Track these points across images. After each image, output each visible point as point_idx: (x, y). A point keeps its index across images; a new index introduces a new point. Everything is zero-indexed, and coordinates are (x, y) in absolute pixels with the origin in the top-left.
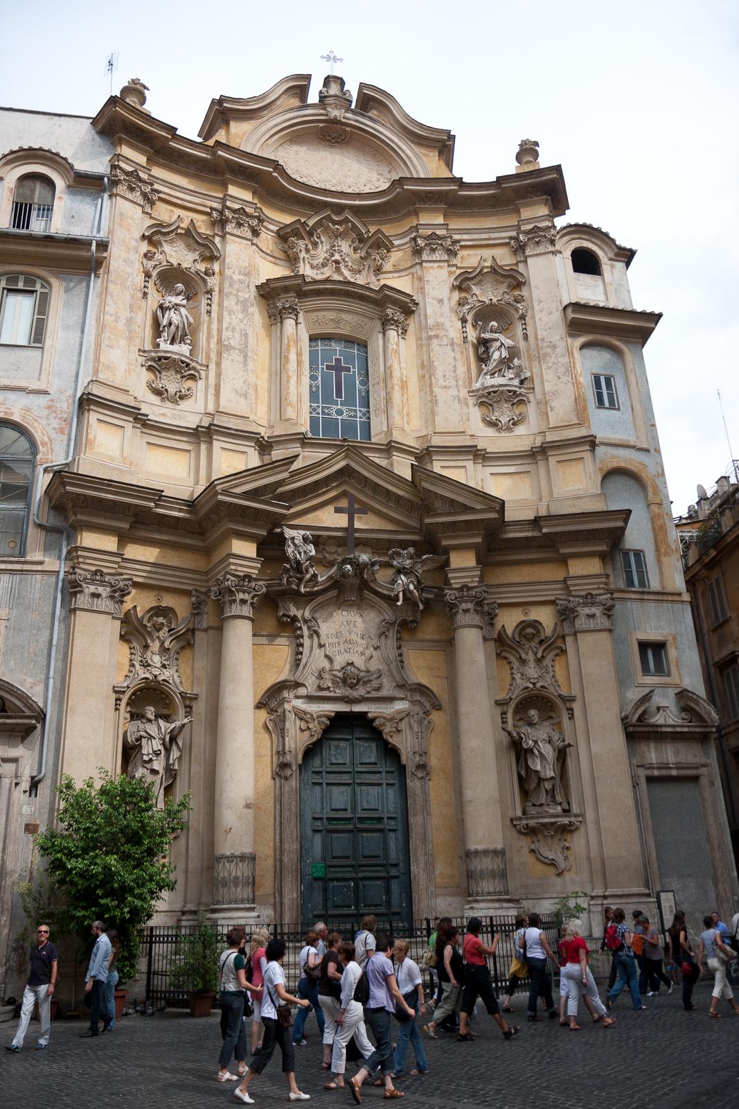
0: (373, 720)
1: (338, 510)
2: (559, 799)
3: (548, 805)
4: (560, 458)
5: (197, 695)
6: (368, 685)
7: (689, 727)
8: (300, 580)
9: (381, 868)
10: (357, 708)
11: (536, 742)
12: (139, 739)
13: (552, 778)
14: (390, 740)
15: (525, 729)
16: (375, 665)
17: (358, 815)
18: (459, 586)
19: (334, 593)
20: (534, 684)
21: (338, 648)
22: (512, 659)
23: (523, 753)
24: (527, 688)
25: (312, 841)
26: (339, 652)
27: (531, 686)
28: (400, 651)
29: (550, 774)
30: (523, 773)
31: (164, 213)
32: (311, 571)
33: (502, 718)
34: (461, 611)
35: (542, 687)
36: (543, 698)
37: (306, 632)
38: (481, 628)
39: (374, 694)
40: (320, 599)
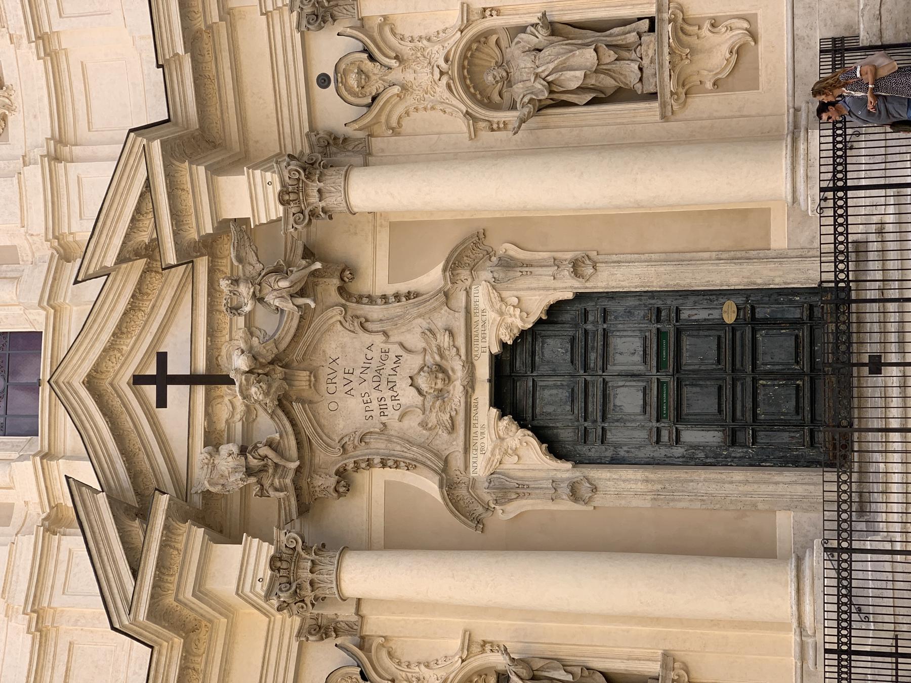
0: (504, 345)
1: (162, 402)
2: (632, 37)
3: (641, 58)
4: (54, 10)
5: (465, 631)
6: (447, 353)
8: (276, 465)
9: (738, 334)
10: (483, 371)
11: (537, 76)
13: (596, 50)
14: (533, 318)
15: (518, 89)
16: (414, 340)
17: (654, 371)
18: (281, 208)
19: (297, 409)
20: (442, 73)
21: (389, 402)
22: (400, 110)
23: (555, 96)
24: (449, 87)
25: (696, 447)
26: (394, 398)
27: (445, 79)
28: (392, 299)
29: (589, 56)
30: (589, 97)
32: (264, 451)
33: (499, 129)
34: (322, 204)
35: (446, 60)
36: (465, 57)
37: (362, 452)
38: (351, 166)
39: (461, 341)
40: (308, 429)
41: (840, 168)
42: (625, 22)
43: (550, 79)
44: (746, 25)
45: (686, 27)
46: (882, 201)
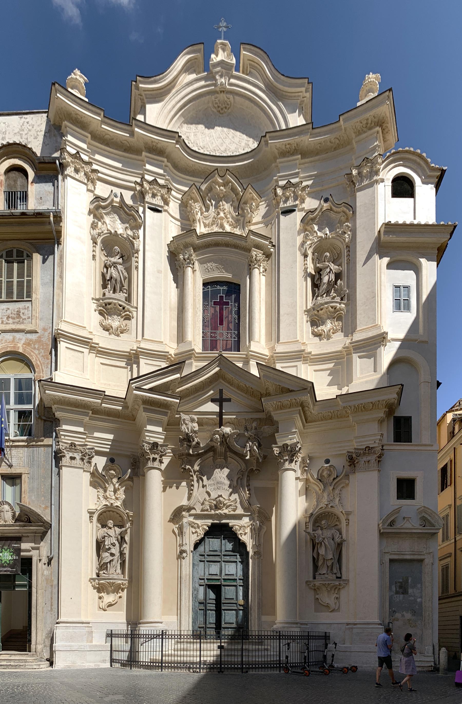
2: (335, 571)
7: (421, 529)
11: (324, 539)
12: (104, 537)
15: (319, 532)
31: (102, 190)
35: (332, 507)
41: (286, 637)
42: (340, 569)
43: (323, 543)
44: (336, 609)
45: (337, 590)
46: (275, 650)
